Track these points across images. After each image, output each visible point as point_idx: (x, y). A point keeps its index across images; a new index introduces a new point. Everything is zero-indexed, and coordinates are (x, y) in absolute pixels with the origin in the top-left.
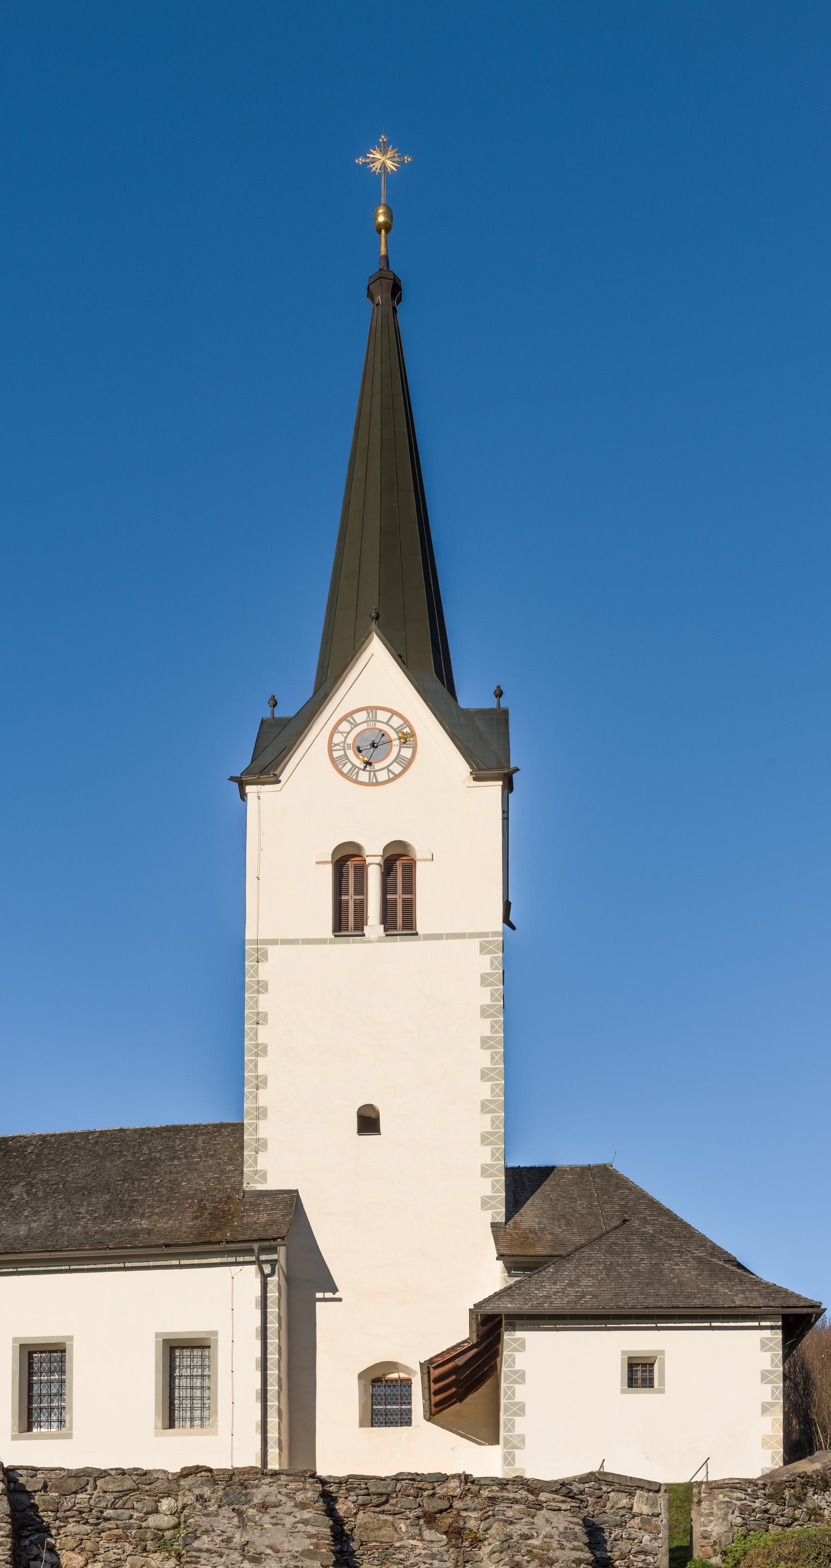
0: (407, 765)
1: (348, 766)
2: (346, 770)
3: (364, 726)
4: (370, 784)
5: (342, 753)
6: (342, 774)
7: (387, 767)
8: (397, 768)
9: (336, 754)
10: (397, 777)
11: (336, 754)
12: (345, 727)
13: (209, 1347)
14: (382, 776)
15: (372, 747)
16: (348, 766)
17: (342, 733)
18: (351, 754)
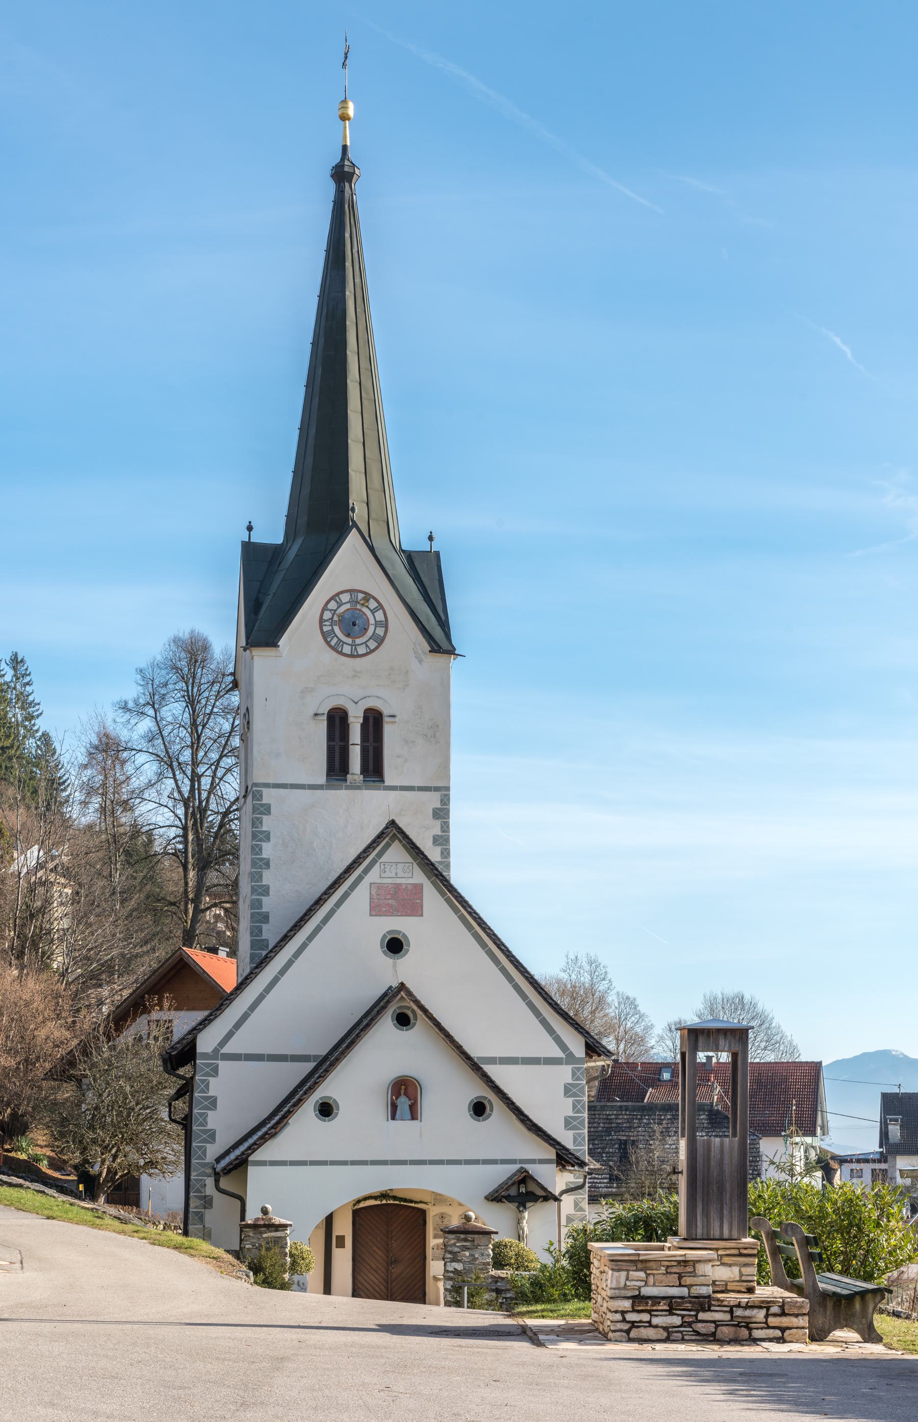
0: (380, 641)
1: (335, 640)
2: (333, 643)
3: (348, 606)
4: (351, 656)
5: (330, 628)
6: (330, 646)
7: (365, 643)
8: (372, 645)
9: (325, 629)
10: (372, 651)
11: (325, 629)
12: (333, 605)
13: (393, 1118)
14: (362, 650)
15: (352, 624)
16: (335, 640)
17: (330, 610)
18: (337, 629)
